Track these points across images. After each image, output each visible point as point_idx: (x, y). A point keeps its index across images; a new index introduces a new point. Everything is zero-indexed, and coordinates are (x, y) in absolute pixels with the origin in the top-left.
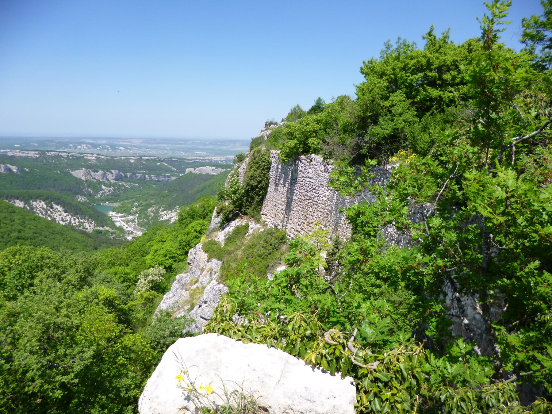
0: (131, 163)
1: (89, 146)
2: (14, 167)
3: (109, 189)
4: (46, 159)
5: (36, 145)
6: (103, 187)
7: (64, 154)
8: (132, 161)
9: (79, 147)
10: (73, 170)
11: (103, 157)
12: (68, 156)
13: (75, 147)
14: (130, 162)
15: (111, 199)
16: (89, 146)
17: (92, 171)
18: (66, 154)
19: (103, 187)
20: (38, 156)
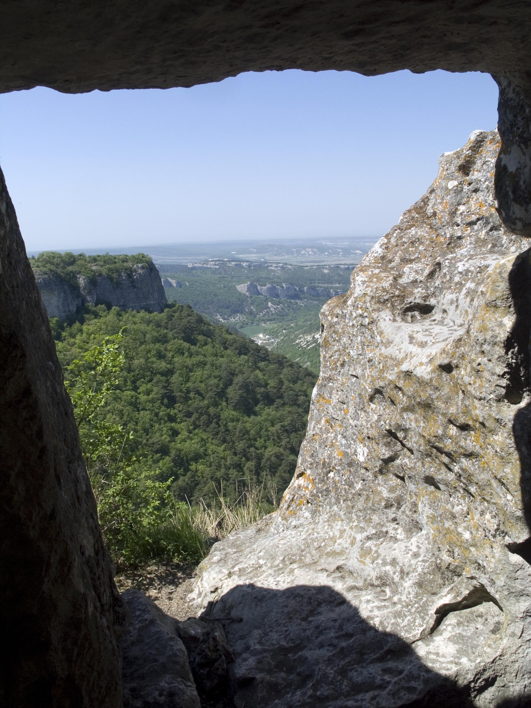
0: (324, 275)
1: (315, 250)
2: (174, 281)
3: (275, 307)
4: (225, 271)
5: (255, 251)
6: (270, 304)
7: (244, 264)
8: (326, 271)
9: (303, 252)
10: (239, 285)
11: (289, 267)
12: (249, 266)
13: (299, 252)
14: (323, 273)
15: (274, 319)
16: (315, 250)
17: (259, 285)
18: (247, 264)
19: (270, 304)
20: (217, 267)
